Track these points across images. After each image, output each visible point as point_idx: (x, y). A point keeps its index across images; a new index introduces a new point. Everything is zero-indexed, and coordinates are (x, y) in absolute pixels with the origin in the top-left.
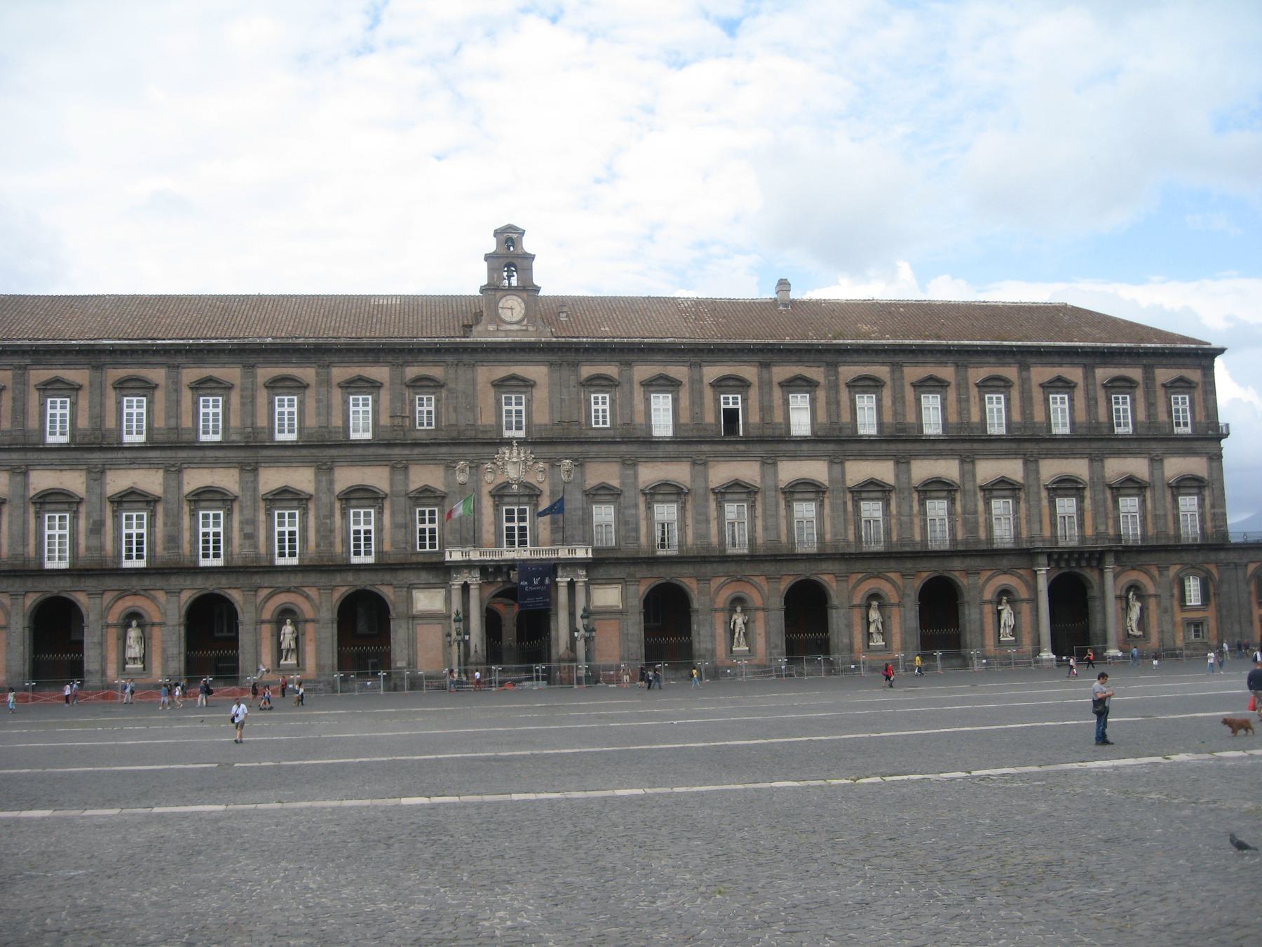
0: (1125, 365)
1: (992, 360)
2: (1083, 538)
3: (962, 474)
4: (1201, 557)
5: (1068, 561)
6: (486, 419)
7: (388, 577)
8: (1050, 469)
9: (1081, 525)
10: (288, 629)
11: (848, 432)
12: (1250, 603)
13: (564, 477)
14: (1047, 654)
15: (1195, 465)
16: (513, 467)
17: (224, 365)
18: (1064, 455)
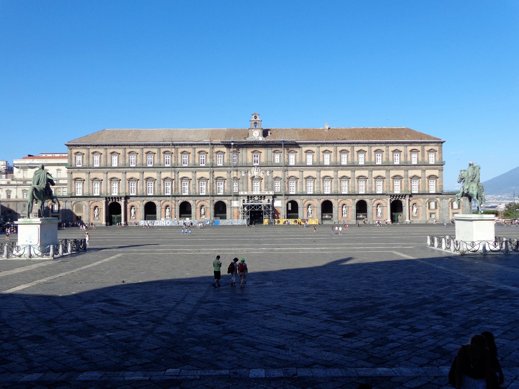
0: (416, 146)
1: (378, 145)
2: (401, 191)
3: (369, 174)
4: (435, 196)
5: (396, 197)
6: (250, 160)
7: (225, 198)
8: (393, 173)
9: (401, 188)
10: (203, 210)
11: (338, 164)
12: (449, 209)
13: (268, 175)
14: (389, 220)
15: (436, 173)
16: (255, 172)
17: (188, 148)
18: (397, 169)
